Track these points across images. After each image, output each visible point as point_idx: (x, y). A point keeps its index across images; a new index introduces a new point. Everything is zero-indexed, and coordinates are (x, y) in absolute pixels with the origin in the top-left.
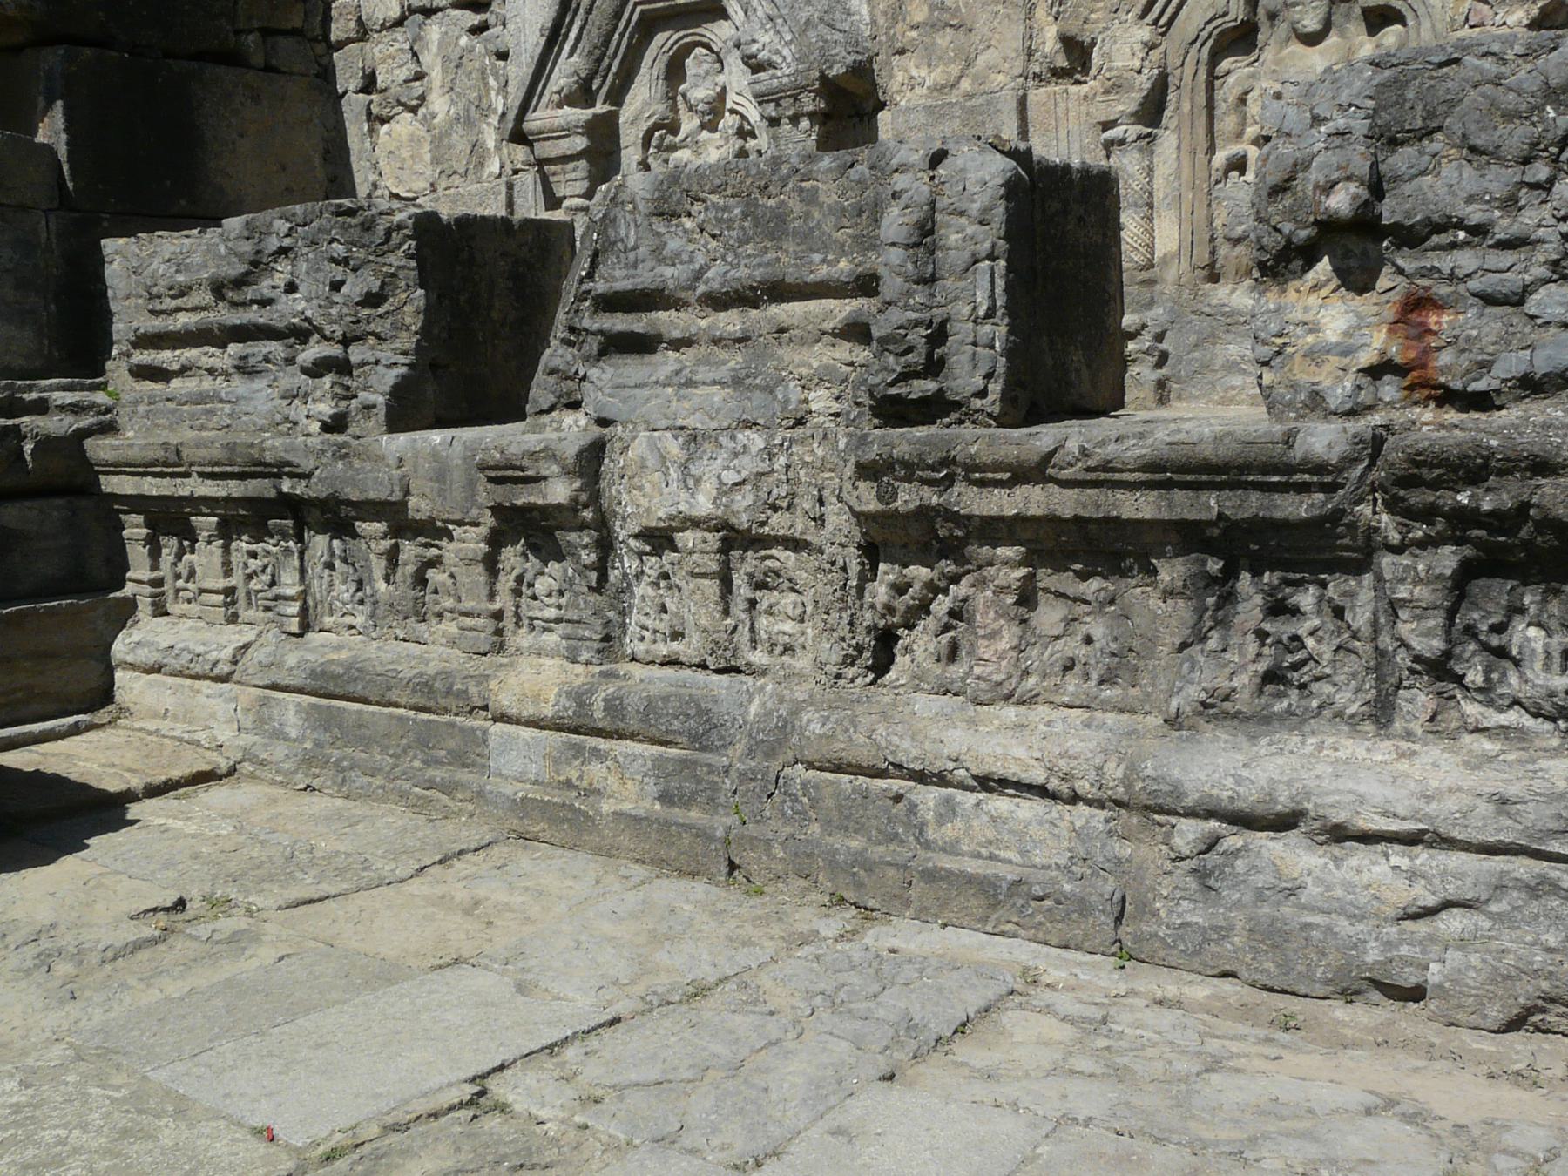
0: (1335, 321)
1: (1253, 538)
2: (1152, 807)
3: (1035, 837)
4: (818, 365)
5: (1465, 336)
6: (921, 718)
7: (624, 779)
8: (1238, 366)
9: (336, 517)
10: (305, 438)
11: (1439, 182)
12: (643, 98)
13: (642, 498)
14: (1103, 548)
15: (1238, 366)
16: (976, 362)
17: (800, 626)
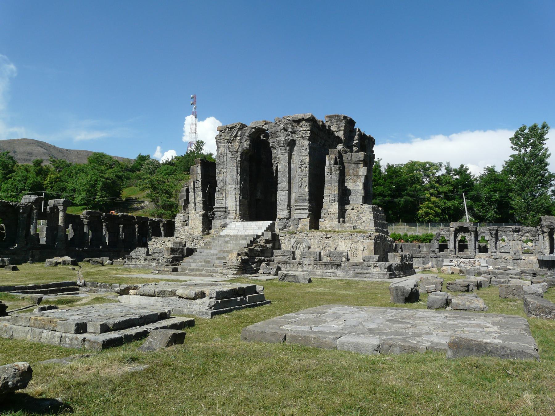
0: (329, 258)
1: (326, 264)
2: (323, 272)
3: (320, 273)
4: (312, 258)
6: (315, 270)
8: (325, 259)
9: (289, 263)
10: (287, 260)
11: (331, 255)
12: (299, 245)
13: (304, 263)
14: (322, 265)
15: (325, 259)
16: (318, 259)
17: (311, 268)
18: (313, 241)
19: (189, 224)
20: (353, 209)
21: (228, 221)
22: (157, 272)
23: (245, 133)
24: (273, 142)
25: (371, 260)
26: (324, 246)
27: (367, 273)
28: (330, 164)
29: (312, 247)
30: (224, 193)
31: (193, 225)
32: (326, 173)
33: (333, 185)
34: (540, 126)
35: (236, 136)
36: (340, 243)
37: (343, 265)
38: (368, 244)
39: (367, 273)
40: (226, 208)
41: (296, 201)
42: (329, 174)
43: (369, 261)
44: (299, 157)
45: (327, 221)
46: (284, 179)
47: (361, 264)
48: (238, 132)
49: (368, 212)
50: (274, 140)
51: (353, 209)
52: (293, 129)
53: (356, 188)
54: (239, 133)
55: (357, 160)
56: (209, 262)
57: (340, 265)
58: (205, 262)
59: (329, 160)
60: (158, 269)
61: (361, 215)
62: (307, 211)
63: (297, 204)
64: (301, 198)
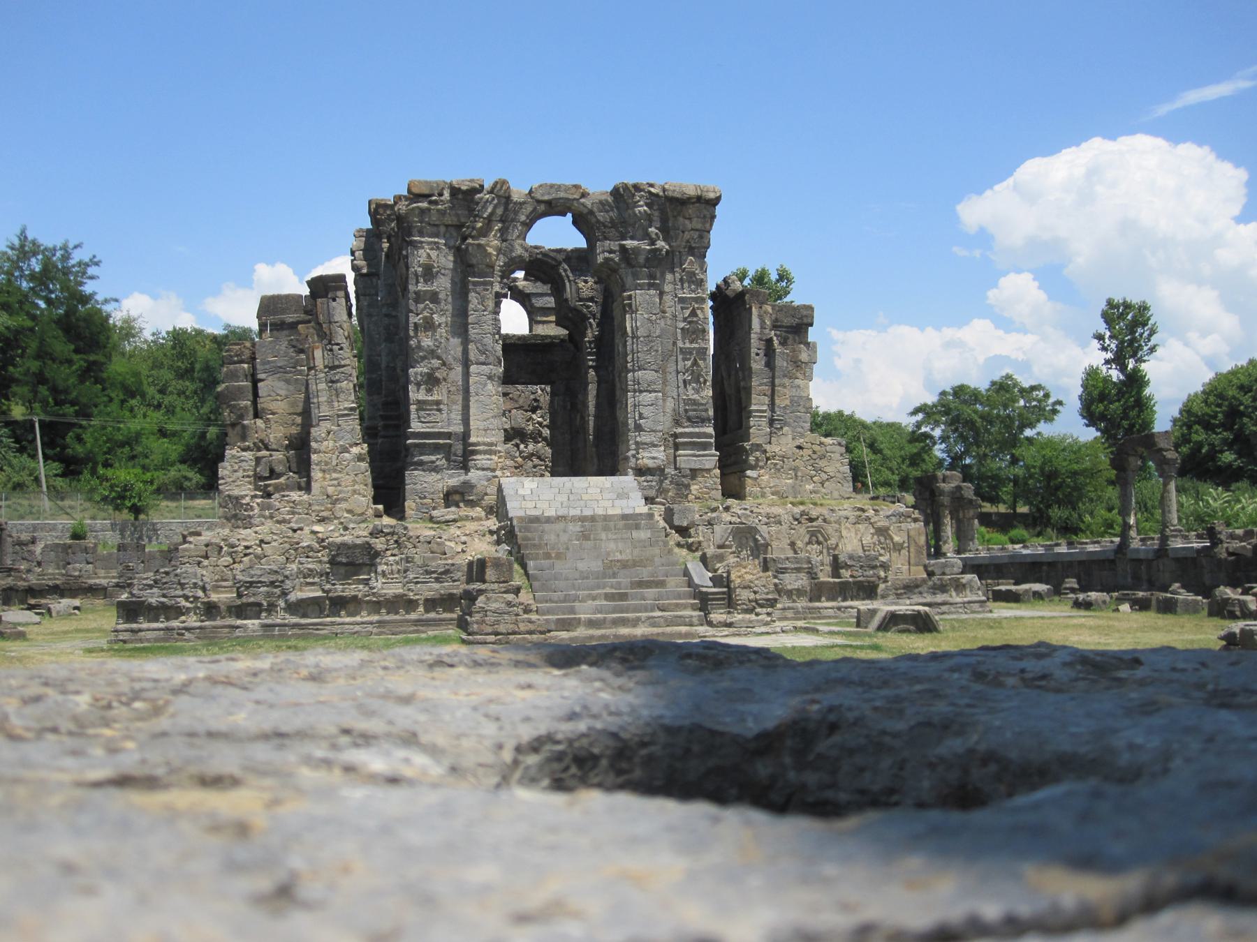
5: (855, 573)
7: (790, 614)
18: (774, 528)
19: (315, 486)
20: (799, 447)
21: (474, 476)
22: (492, 638)
23: (516, 213)
24: (611, 252)
25: (947, 570)
26: (807, 539)
27: (944, 604)
28: (762, 327)
29: (774, 544)
30: (445, 391)
31: (330, 490)
32: (754, 351)
33: (777, 381)
34: (774, 277)
35: (489, 221)
36: (844, 533)
37: (882, 586)
38: (912, 533)
39: (944, 604)
40: (448, 435)
41: (677, 423)
42: (762, 352)
43: (944, 574)
44: (682, 300)
45: (766, 478)
46: (649, 358)
47: (924, 581)
48: (495, 207)
49: (837, 456)
50: (614, 245)
51: (799, 447)
52: (664, 221)
53: (794, 392)
54: (500, 211)
55: (795, 321)
56: (623, 597)
57: (876, 586)
58: (608, 597)
59: (760, 317)
60: (490, 630)
61: (822, 463)
62: (714, 452)
63: (680, 430)
64: (691, 413)
